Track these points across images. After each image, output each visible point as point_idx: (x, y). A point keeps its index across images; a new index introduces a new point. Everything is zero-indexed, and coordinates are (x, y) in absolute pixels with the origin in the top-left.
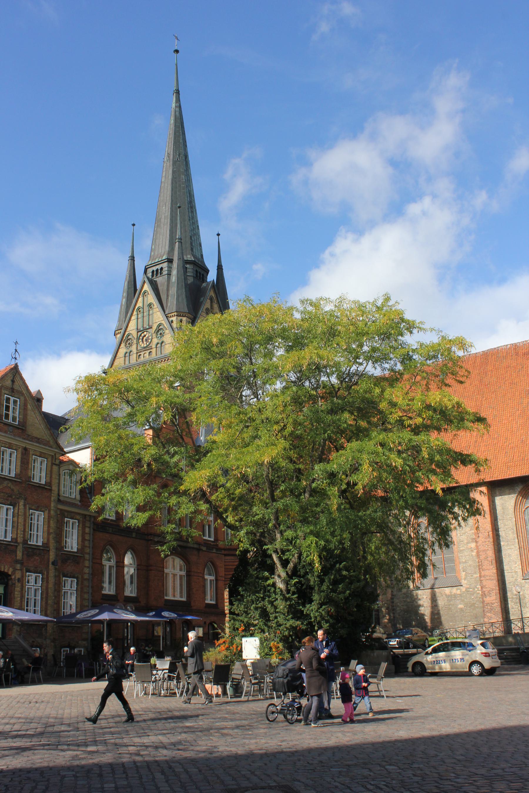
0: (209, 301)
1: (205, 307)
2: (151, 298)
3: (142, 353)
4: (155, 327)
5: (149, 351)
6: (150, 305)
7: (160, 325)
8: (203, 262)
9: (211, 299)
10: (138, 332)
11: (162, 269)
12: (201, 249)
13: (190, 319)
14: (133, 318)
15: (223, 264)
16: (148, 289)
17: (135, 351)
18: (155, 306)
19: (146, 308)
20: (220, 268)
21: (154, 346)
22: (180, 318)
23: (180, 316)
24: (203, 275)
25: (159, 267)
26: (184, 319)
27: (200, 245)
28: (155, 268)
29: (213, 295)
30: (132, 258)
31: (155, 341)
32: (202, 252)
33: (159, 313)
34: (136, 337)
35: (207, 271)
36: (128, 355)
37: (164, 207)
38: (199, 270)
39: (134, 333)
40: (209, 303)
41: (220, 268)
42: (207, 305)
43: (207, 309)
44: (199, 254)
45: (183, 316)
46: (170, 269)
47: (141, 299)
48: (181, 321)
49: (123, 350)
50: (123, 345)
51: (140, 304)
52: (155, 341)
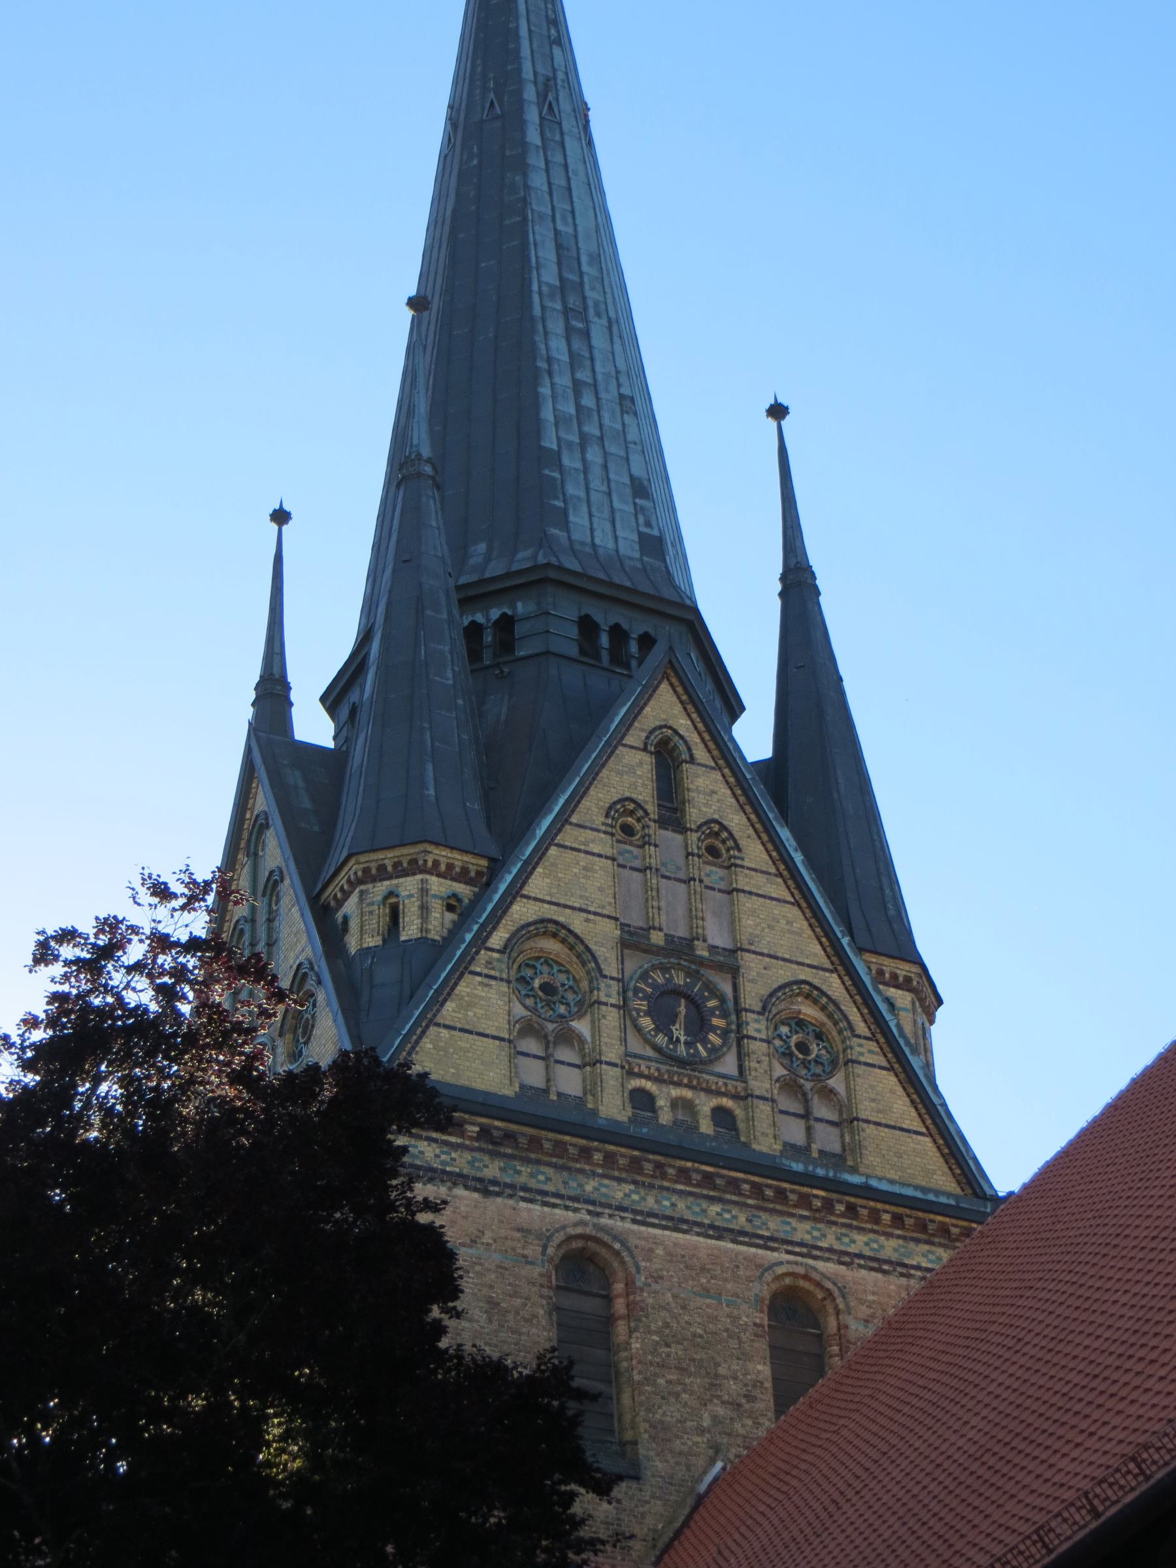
13: (463, 876)
20: (798, 586)
22: (383, 887)
26: (408, 886)
29: (683, 724)
30: (273, 692)
38: (605, 617)
41: (798, 586)
43: (624, 807)
45: (401, 871)
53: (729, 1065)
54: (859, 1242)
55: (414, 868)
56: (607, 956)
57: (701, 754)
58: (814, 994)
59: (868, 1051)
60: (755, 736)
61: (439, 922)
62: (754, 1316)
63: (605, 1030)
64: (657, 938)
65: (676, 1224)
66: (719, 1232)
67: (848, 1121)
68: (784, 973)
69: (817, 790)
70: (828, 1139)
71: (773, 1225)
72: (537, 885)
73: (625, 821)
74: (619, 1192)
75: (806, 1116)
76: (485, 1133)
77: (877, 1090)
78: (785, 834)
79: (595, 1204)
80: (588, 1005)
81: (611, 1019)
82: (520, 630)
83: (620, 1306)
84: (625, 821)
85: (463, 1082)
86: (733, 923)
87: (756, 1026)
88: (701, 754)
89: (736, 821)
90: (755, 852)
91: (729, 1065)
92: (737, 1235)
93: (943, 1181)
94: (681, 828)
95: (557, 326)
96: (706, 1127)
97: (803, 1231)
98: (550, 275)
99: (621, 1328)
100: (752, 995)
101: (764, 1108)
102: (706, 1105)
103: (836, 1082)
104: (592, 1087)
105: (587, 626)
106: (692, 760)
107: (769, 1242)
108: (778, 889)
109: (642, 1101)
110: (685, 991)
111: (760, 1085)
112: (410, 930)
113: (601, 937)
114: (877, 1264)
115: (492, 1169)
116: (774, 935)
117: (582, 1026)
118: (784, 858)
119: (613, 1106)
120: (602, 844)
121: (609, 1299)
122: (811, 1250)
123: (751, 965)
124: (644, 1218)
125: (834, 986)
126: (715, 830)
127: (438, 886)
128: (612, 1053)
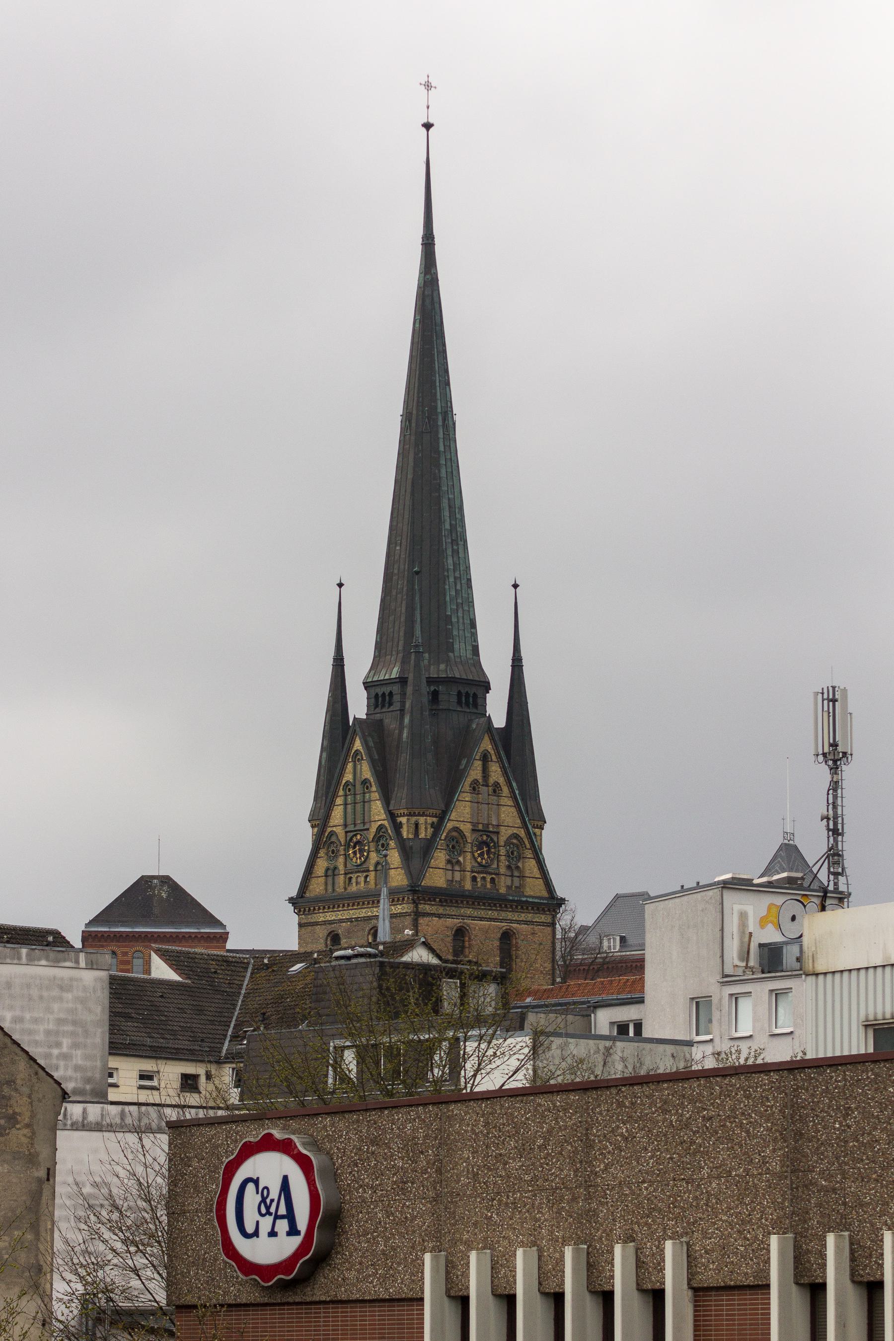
0: (478, 764)
1: (469, 780)
2: (366, 771)
3: (354, 876)
4: (374, 828)
5: (365, 874)
6: (365, 782)
7: (381, 827)
8: (478, 665)
9: (485, 758)
10: (346, 832)
11: (391, 694)
12: (474, 635)
14: (339, 801)
15: (523, 654)
16: (360, 748)
17: (341, 867)
18: (374, 788)
19: (359, 787)
21: (372, 868)
22: (414, 819)
23: (414, 815)
24: (475, 694)
25: (387, 690)
26: (422, 820)
27: (473, 625)
28: (380, 691)
31: (374, 857)
32: (476, 640)
33: (378, 803)
34: (343, 841)
35: (487, 687)
36: (330, 873)
37: (398, 548)
39: (340, 831)
40: (480, 768)
42: (475, 772)
43: (475, 782)
44: (470, 648)
45: (419, 815)
46: (403, 694)
47: (350, 766)
48: (417, 825)
49: (322, 865)
50: (322, 853)
51: (348, 777)
52: (374, 857)
53: (495, 866)
54: (523, 917)
55: (423, 815)
56: (468, 834)
57: (494, 758)
58: (516, 836)
59: (529, 854)
60: (499, 720)
61: (430, 831)
62: (497, 943)
63: (467, 861)
64: (480, 827)
65: (481, 919)
66: (490, 919)
67: (522, 877)
68: (510, 832)
69: (515, 742)
70: (517, 882)
71: (503, 915)
72: (453, 816)
73: (475, 787)
74: (469, 911)
75: (512, 876)
76: (440, 901)
77: (530, 865)
78: (514, 784)
79: (463, 916)
80: (462, 852)
81: (469, 856)
82: (441, 697)
83: (467, 944)
84: (475, 787)
85: (435, 885)
86: (498, 815)
87: (503, 851)
88: (494, 758)
89: (501, 780)
90: (506, 791)
91: (495, 866)
92: (494, 920)
93: (545, 894)
94: (487, 786)
95: (449, 552)
96: (489, 886)
97: (510, 915)
98: (447, 526)
99: (467, 950)
100: (502, 843)
101: (503, 877)
102: (489, 878)
103: (520, 865)
104: (463, 879)
105: (459, 694)
106: (492, 761)
107: (501, 921)
108: (510, 803)
109: (474, 879)
110: (486, 837)
111: (503, 870)
112: (422, 836)
113: (466, 828)
114: (526, 922)
115: (441, 910)
116: (508, 818)
117: (461, 859)
118: (513, 792)
119: (468, 885)
120: (467, 797)
121: (464, 941)
122: (511, 921)
123: (503, 830)
124: (474, 918)
125: (522, 833)
126: (497, 785)
127: (430, 820)
128: (468, 869)
